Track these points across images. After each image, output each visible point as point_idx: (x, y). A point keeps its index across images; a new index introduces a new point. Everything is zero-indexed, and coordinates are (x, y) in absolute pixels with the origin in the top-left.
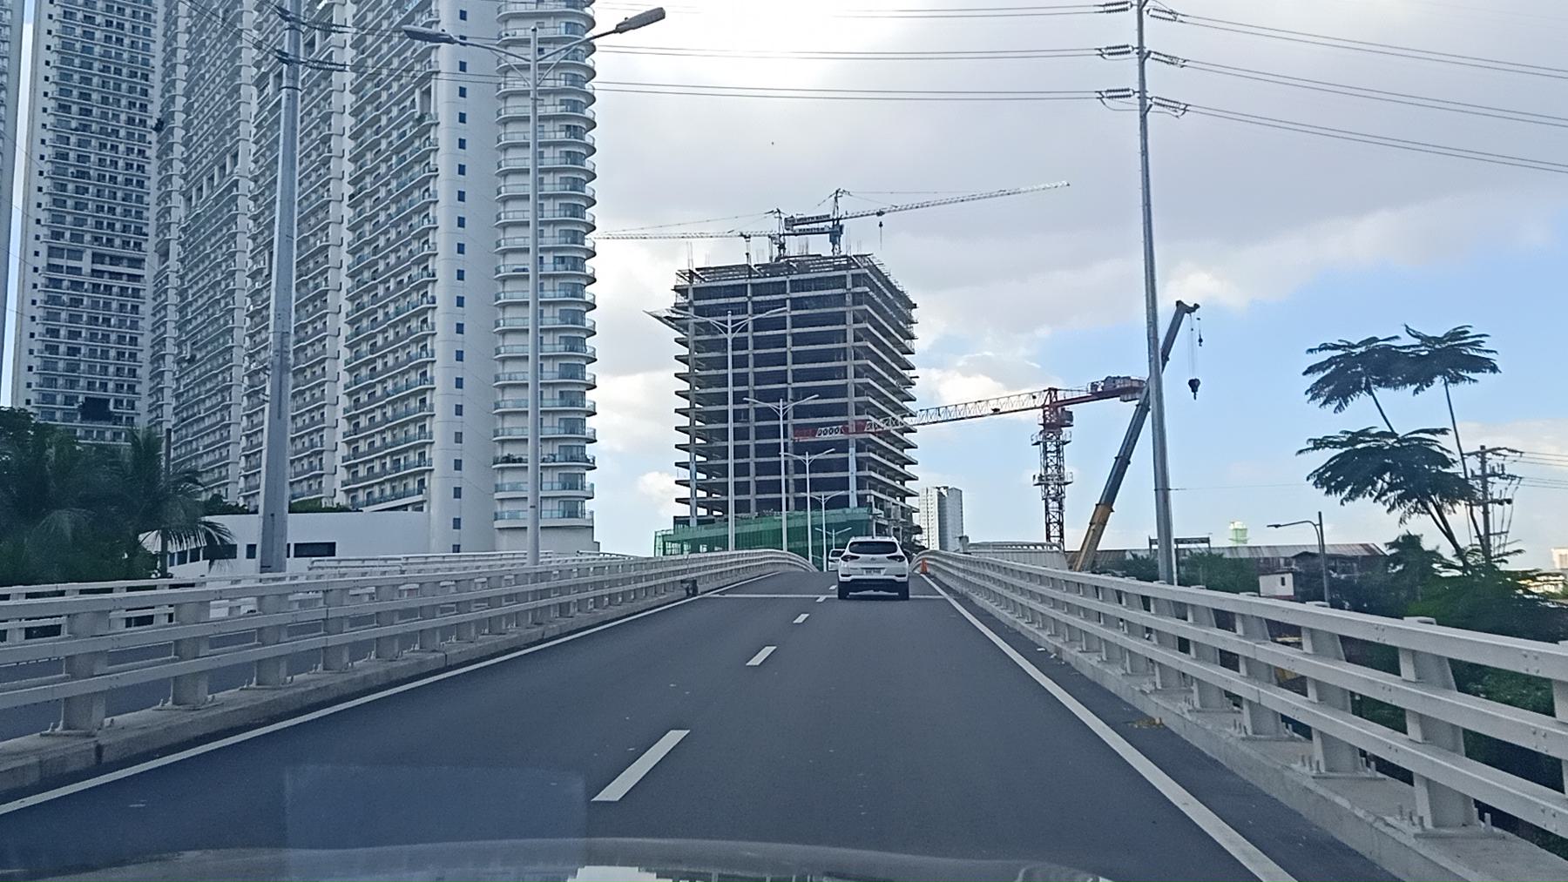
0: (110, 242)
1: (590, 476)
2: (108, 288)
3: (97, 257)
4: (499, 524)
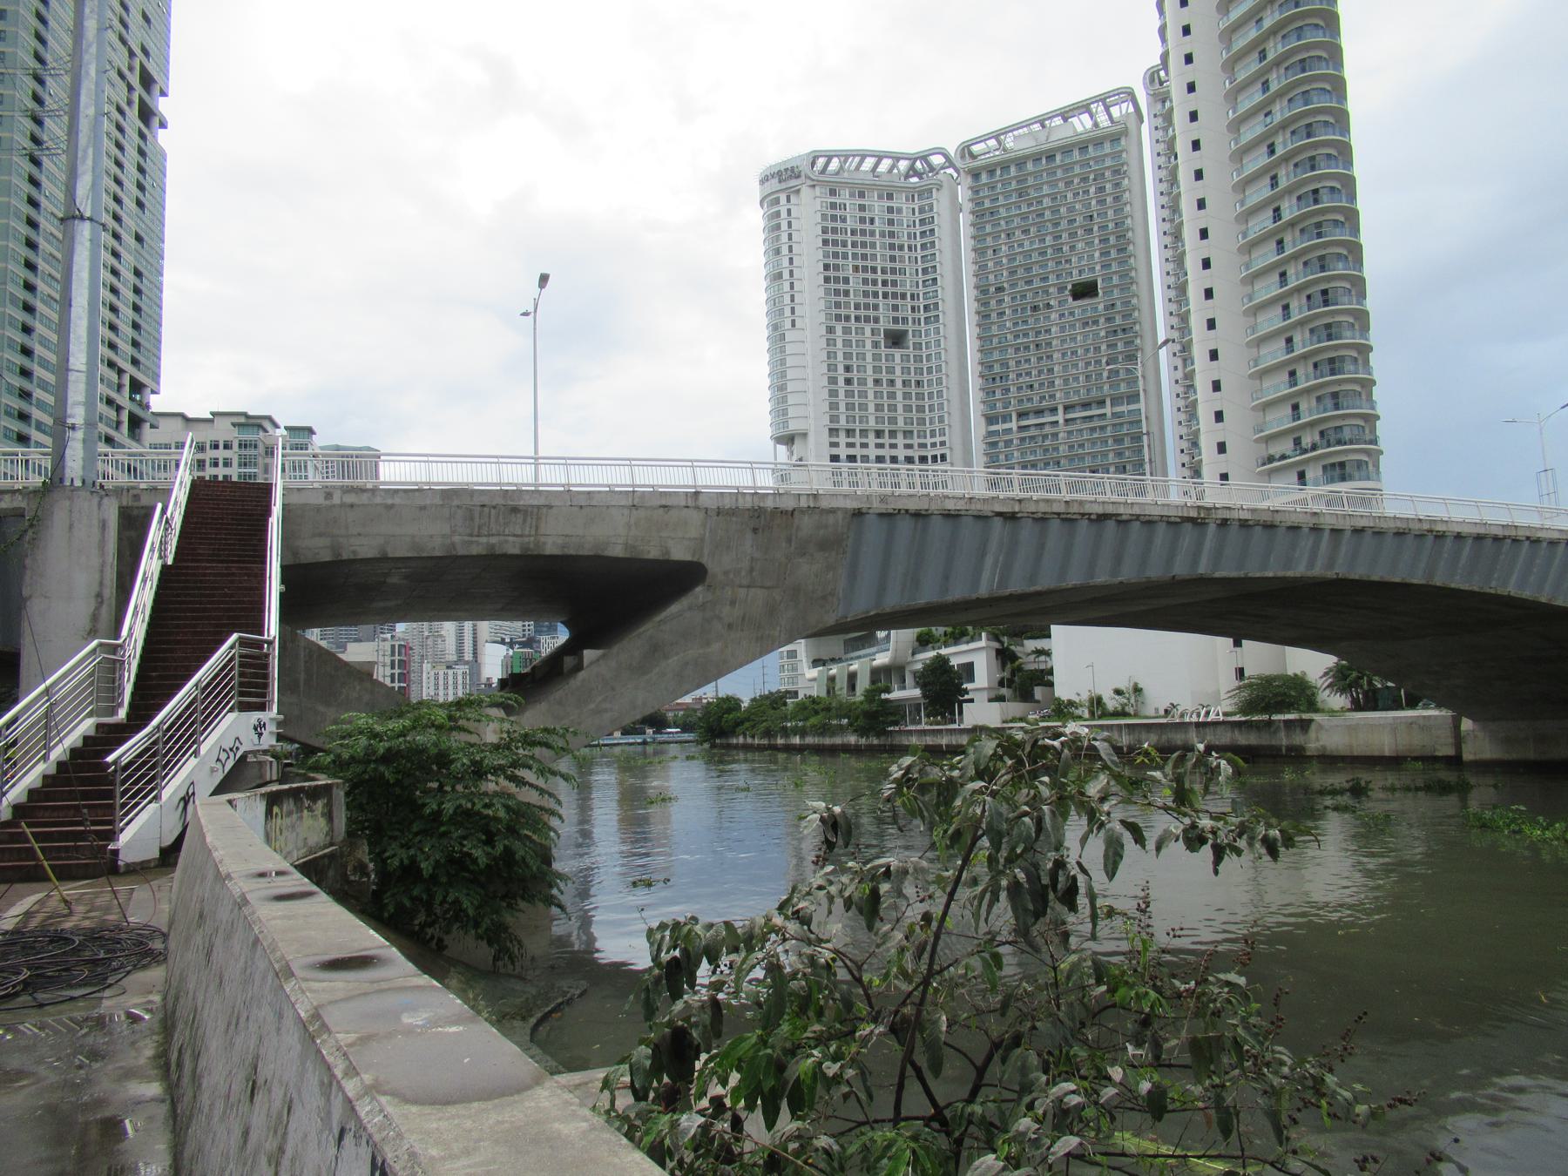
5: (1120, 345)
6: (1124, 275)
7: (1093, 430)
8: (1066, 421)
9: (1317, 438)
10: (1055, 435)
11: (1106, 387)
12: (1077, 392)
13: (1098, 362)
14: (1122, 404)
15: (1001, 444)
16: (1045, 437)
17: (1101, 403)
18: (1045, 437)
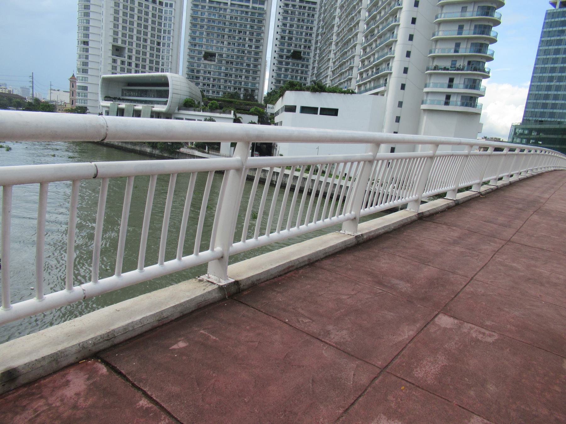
1: (484, 83)
2: (305, 7)
4: (423, 107)
7: (242, 12)
8: (231, 4)
9: (466, 64)
10: (225, 10)
14: (257, 3)
15: (200, 7)
16: (221, 9)
18: (221, 9)
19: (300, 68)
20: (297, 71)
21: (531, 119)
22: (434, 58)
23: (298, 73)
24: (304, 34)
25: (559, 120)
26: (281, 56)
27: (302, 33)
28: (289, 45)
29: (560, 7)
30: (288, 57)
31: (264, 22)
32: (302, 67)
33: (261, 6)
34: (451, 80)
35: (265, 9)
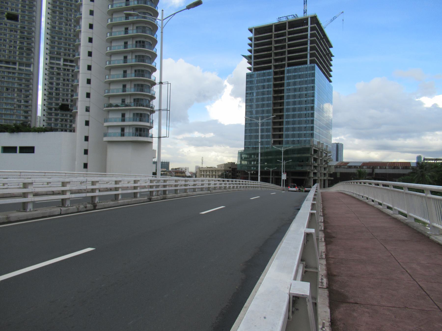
0: (69, 55)
3: (65, 60)
5: (25, 44)
6: (30, 18)
7: (9, 73)
11: (17, 58)
12: (4, 56)
13: (15, 47)
14: (23, 66)
17: (14, 63)
19: (68, 118)
20: (66, 120)
21: (249, 147)
22: (110, 97)
23: (67, 122)
24: (70, 90)
25: (266, 146)
26: (50, 109)
27: (68, 90)
28: (57, 99)
29: (254, 71)
30: (56, 109)
31: (31, 81)
32: (71, 117)
33: (27, 68)
34: (123, 115)
35: (32, 70)
